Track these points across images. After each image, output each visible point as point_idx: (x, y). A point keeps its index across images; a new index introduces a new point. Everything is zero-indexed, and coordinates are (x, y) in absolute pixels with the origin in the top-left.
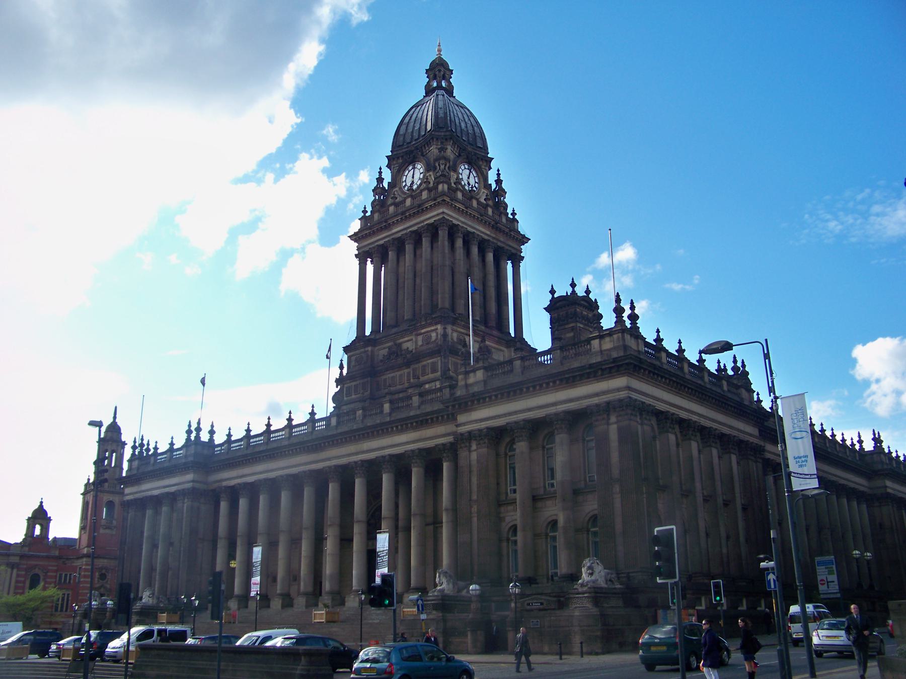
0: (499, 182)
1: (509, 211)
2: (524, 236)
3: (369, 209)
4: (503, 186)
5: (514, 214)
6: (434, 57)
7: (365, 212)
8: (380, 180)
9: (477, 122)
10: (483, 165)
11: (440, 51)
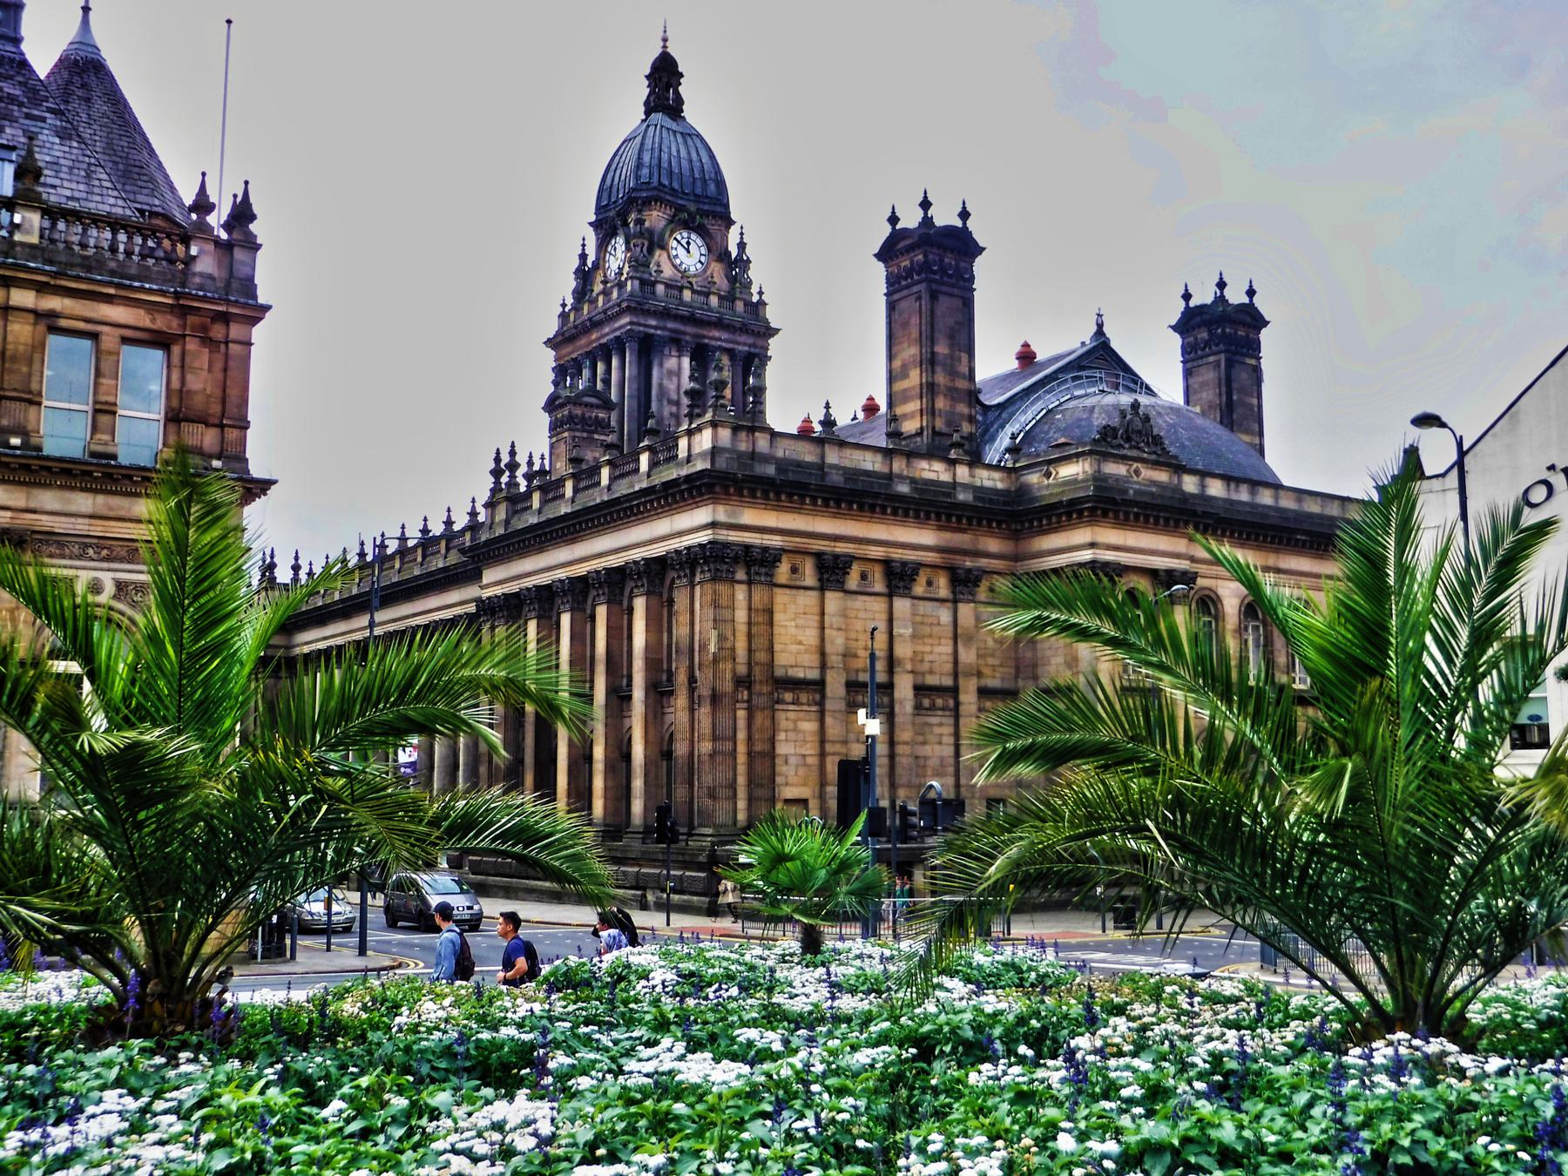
0: (742, 246)
1: (754, 290)
2: (768, 328)
3: (570, 301)
4: (750, 252)
5: (761, 293)
6: (656, 52)
7: (564, 305)
8: (583, 257)
9: (712, 157)
10: (713, 226)
11: (665, 40)
